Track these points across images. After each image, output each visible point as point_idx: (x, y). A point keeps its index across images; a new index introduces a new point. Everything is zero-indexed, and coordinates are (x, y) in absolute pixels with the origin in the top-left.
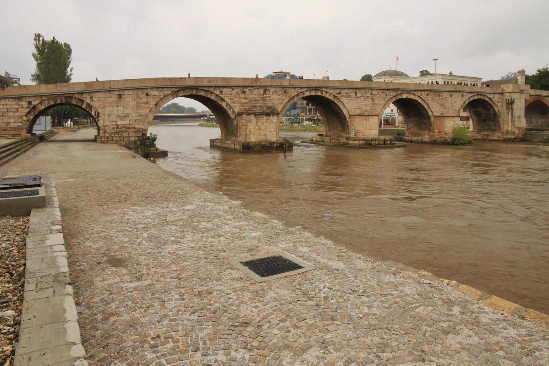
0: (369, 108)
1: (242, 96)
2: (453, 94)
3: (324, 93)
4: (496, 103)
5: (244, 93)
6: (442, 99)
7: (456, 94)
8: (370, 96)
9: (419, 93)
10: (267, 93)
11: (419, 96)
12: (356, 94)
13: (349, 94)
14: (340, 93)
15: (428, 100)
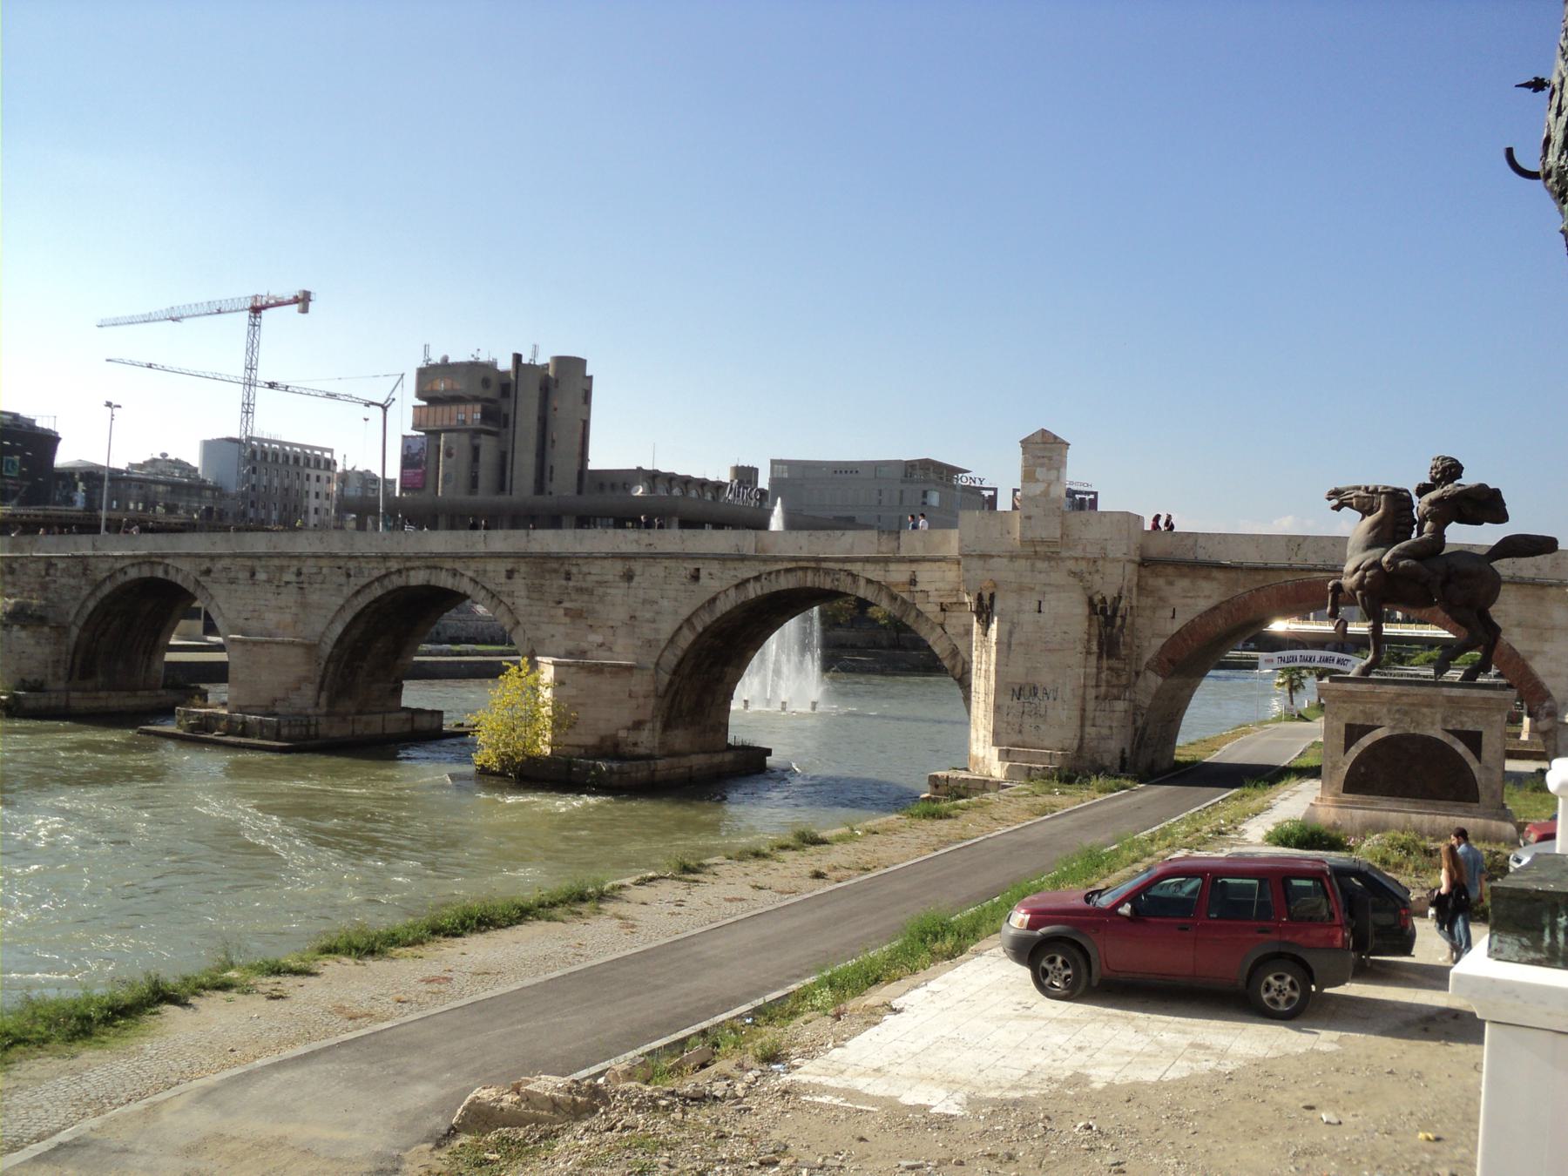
0: (288, 618)
1: (8, 578)
2: (637, 567)
3: (172, 572)
4: (931, 609)
5: (12, 571)
6: (580, 590)
7: (658, 570)
8: (293, 578)
9: (473, 565)
10: (52, 571)
11: (472, 579)
12: (253, 574)
13: (232, 575)
14: (208, 572)
15: (511, 594)
